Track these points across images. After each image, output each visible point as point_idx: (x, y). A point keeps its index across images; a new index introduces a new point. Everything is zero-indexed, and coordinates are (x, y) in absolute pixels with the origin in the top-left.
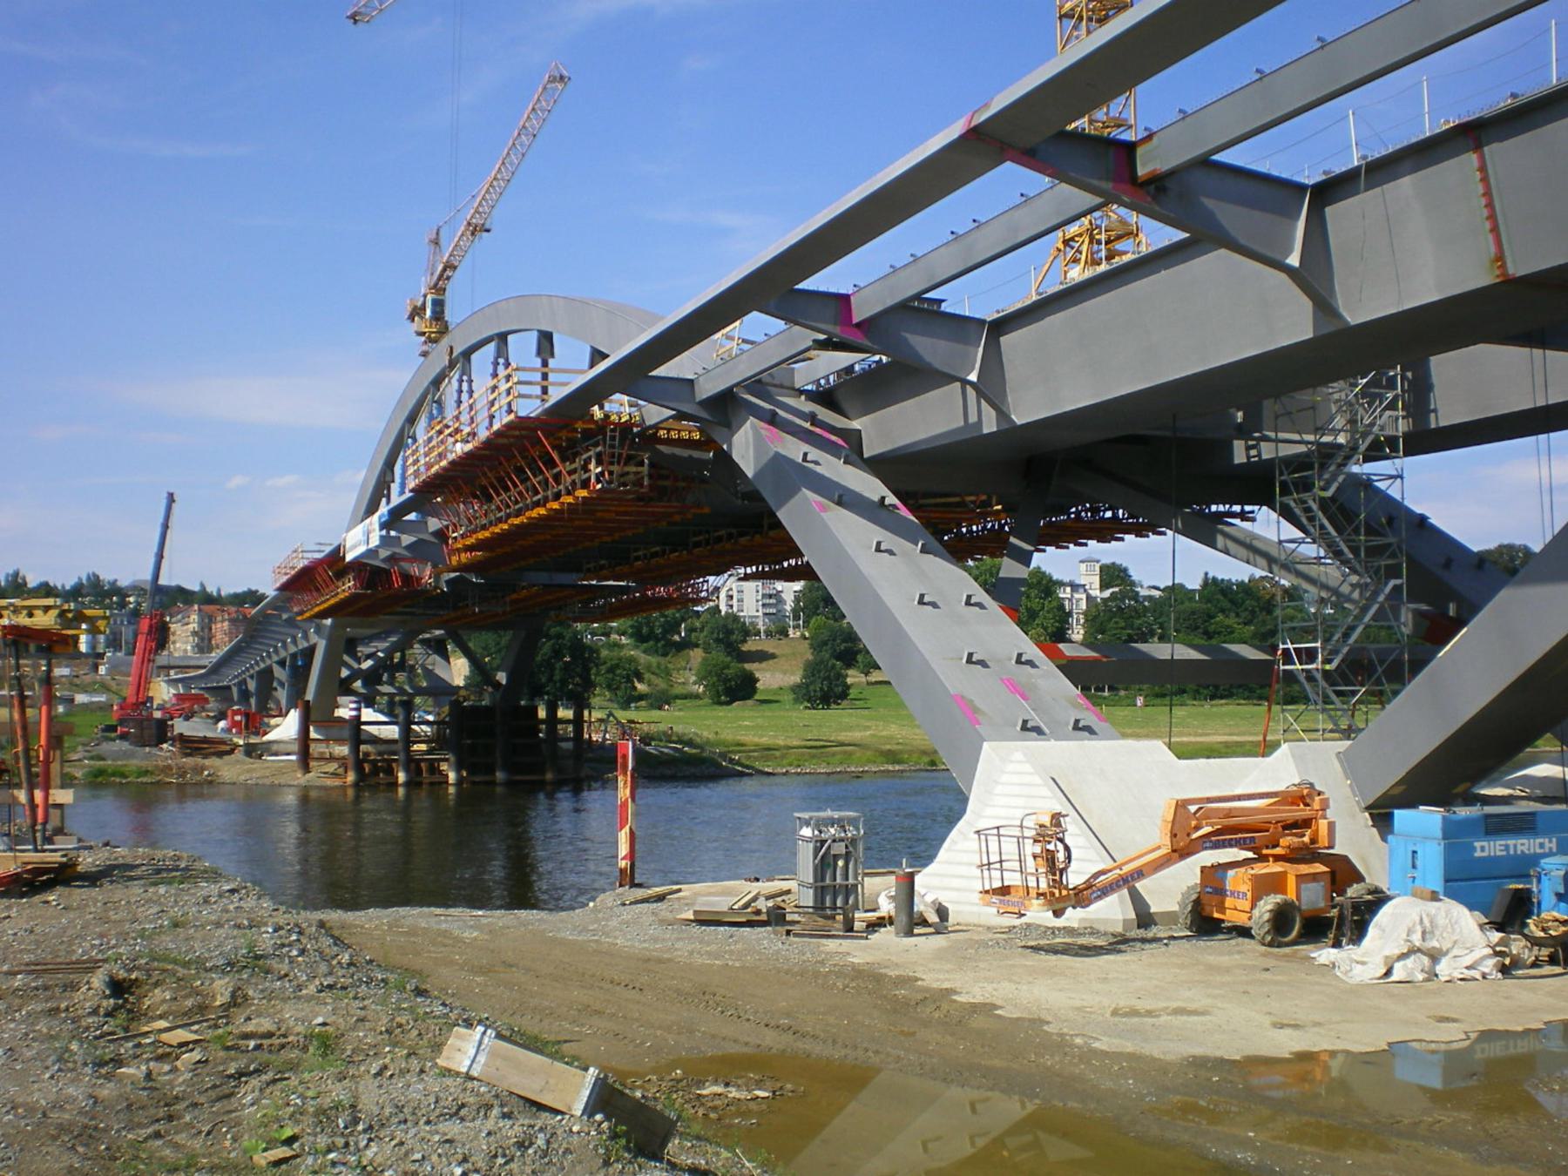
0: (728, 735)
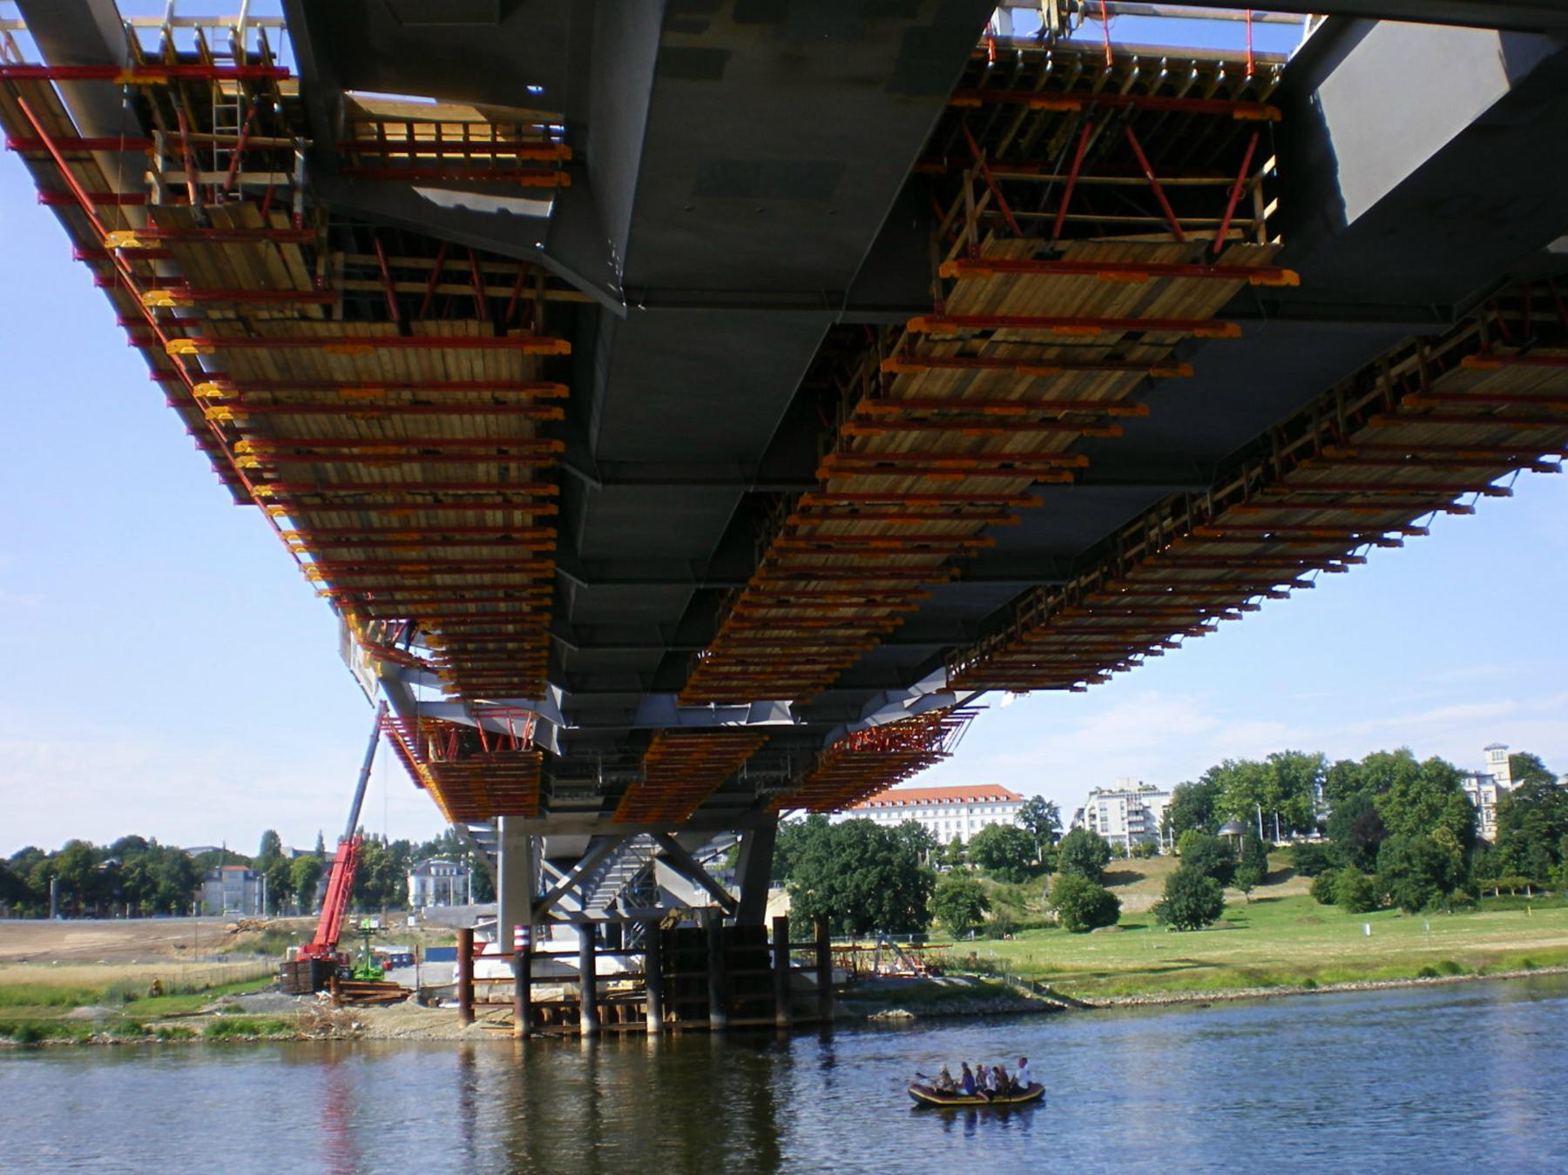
0: (1042, 962)
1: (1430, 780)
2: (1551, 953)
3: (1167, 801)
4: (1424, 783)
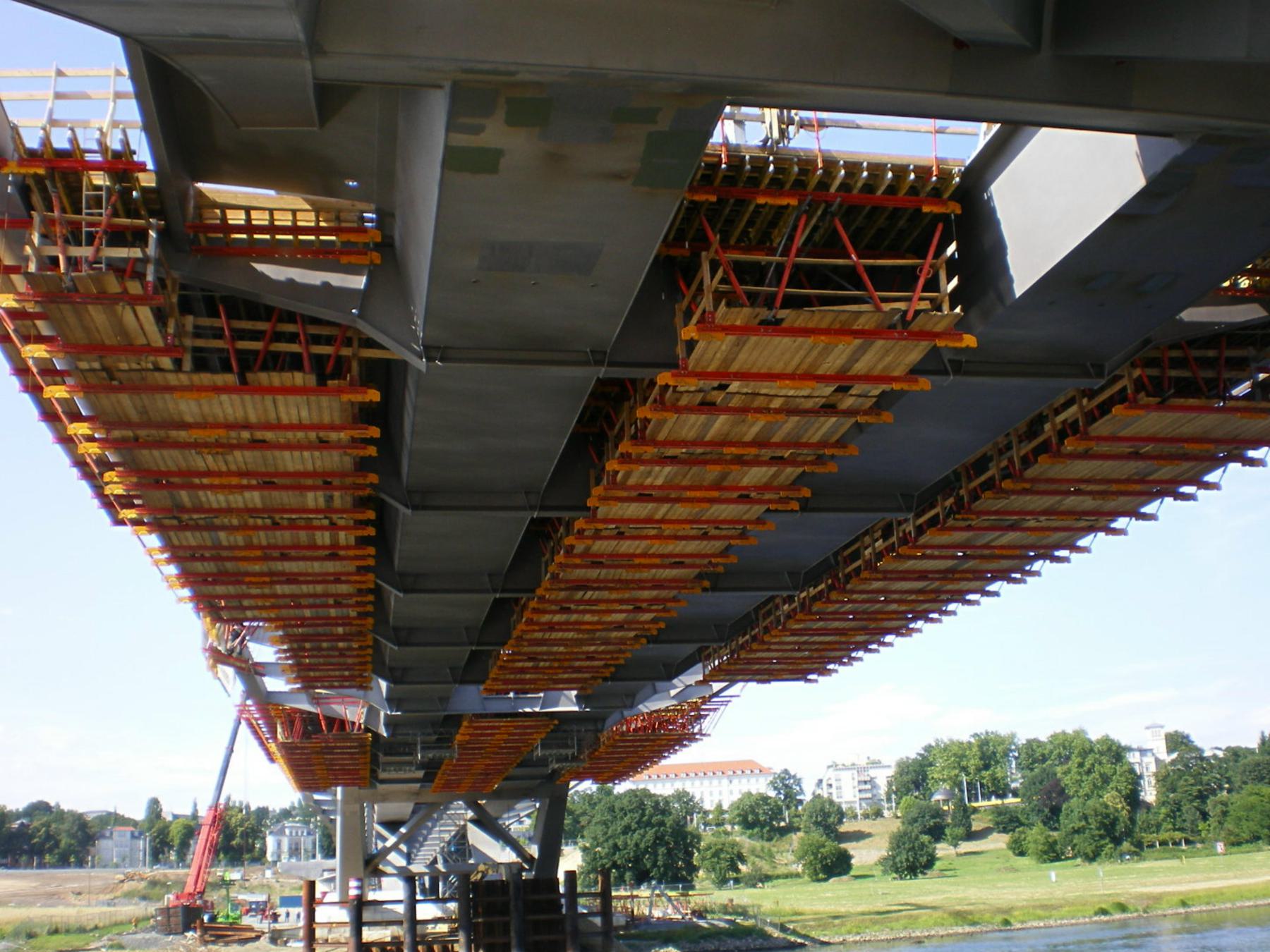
0: (786, 906)
1: (1101, 753)
2: (1201, 894)
3: (891, 772)
4: (1097, 756)
